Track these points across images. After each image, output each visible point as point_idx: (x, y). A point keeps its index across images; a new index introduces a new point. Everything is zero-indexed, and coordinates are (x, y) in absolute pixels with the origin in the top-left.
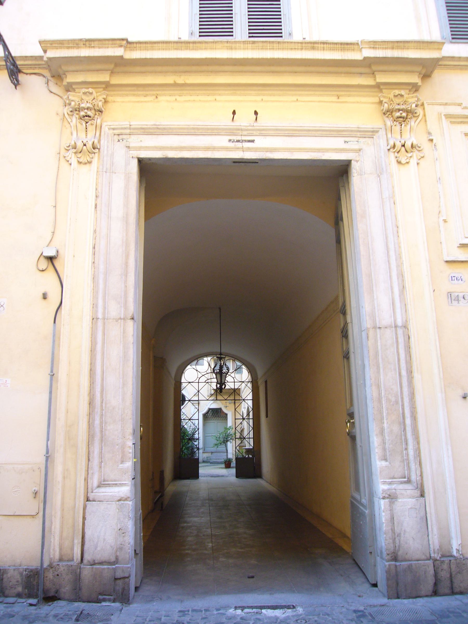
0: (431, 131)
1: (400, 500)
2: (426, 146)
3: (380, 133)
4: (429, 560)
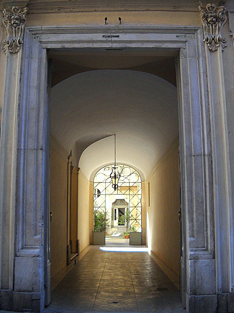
0: (232, 30)
1: (200, 260)
2: (228, 39)
3: (199, 31)
4: (215, 294)
